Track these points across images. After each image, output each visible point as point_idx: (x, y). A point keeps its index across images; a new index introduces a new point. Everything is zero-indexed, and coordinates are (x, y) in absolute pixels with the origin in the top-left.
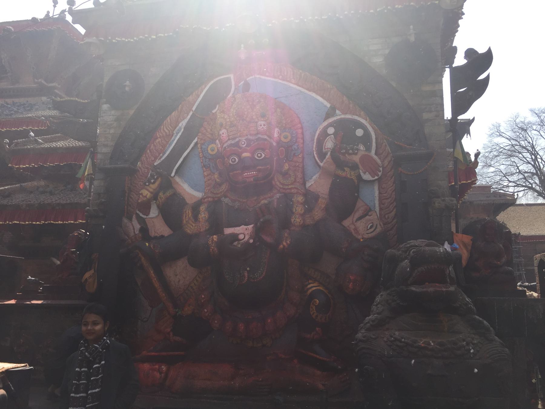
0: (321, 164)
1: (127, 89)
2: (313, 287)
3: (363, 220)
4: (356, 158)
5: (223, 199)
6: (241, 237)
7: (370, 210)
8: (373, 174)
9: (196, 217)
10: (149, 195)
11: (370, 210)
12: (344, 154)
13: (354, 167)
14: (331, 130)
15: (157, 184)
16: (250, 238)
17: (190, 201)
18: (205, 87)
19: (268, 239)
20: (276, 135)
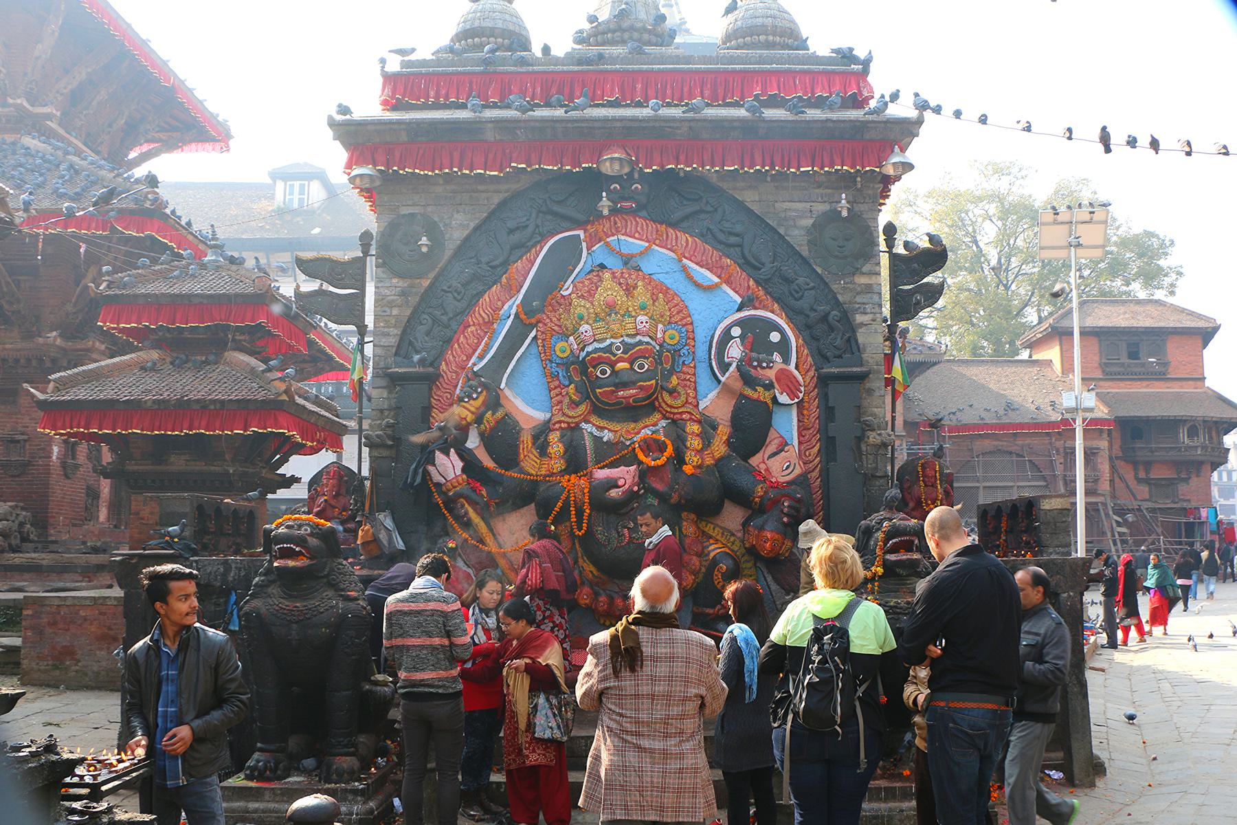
0: (723, 379)
1: (424, 249)
2: (714, 550)
3: (777, 458)
4: (771, 374)
5: (583, 425)
6: (621, 482)
7: (787, 444)
8: (792, 395)
9: (543, 450)
10: (470, 418)
11: (787, 444)
12: (755, 368)
13: (769, 387)
14: (736, 331)
15: (481, 399)
16: (634, 485)
17: (526, 426)
18: (542, 248)
19: (659, 486)
20: (659, 335)
